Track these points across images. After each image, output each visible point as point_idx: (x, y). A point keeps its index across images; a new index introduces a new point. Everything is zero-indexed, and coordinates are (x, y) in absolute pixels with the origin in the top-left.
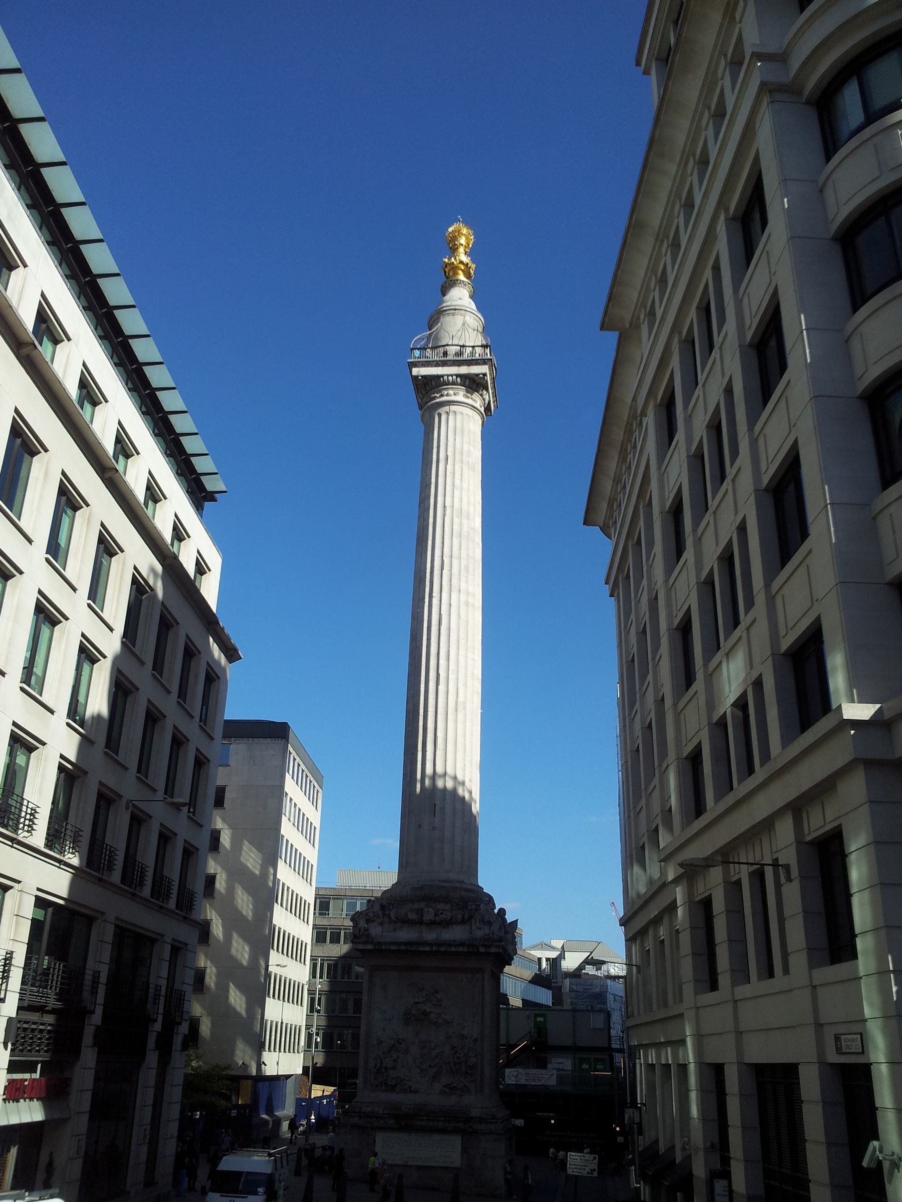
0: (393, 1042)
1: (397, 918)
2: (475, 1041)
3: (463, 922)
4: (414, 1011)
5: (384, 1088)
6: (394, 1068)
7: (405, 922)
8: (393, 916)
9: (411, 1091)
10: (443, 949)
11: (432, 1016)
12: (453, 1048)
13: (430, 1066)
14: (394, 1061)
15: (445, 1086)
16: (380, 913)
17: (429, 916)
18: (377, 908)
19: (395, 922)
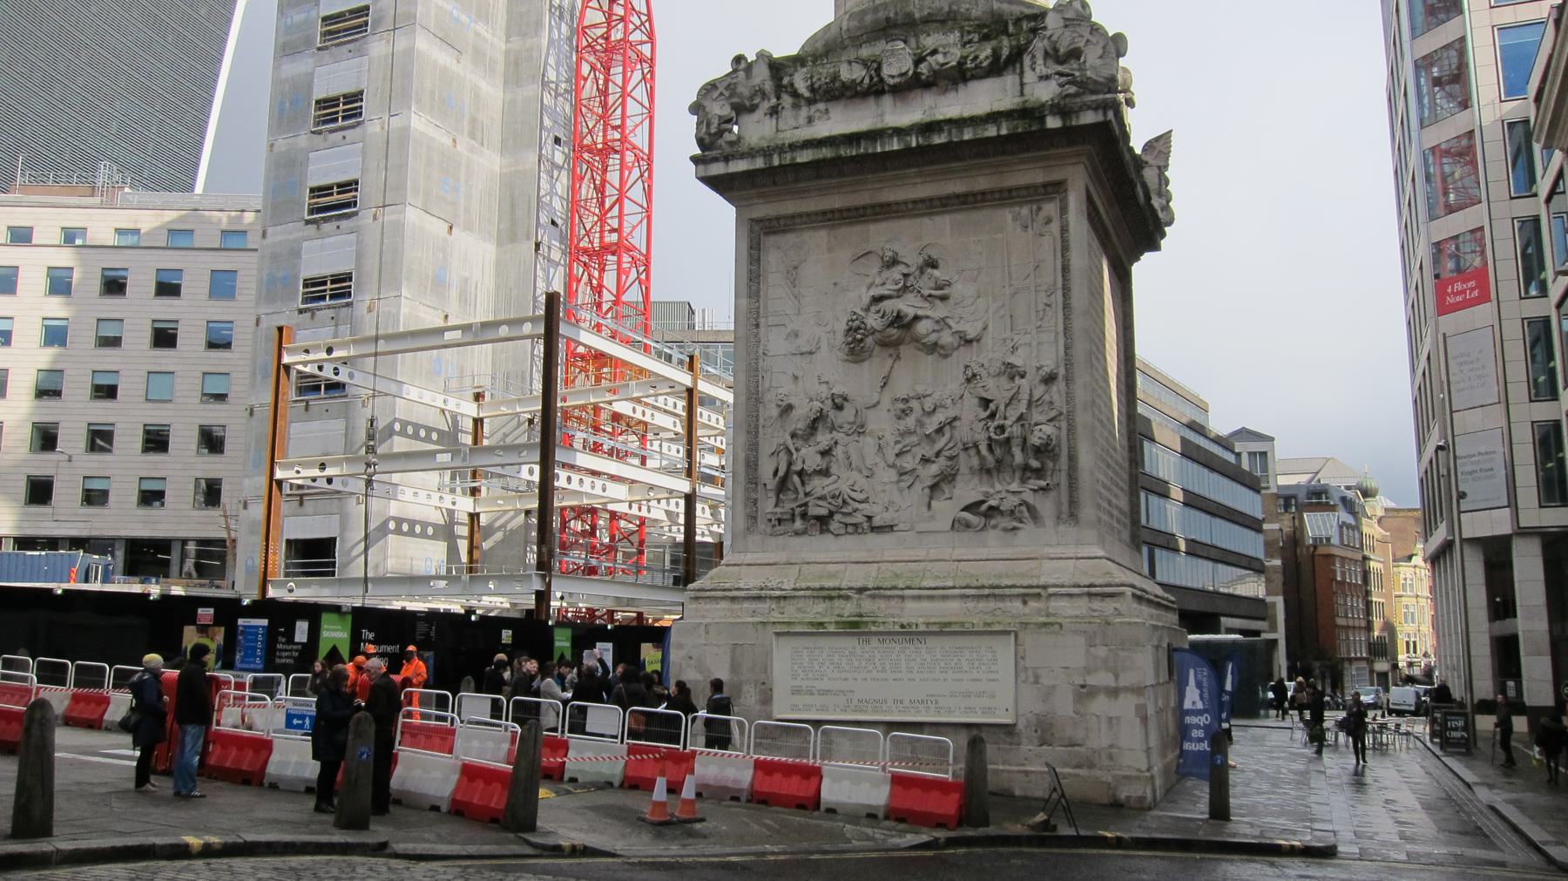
0: (817, 405)
1: (812, 89)
2: (1050, 379)
3: (997, 68)
4: (873, 321)
5: (799, 524)
6: (825, 473)
7: (837, 93)
8: (802, 87)
9: (873, 529)
10: (938, 139)
11: (922, 327)
12: (986, 403)
13: (925, 460)
14: (825, 453)
15: (966, 509)
16: (769, 86)
17: (898, 62)
18: (762, 75)
19: (811, 102)
